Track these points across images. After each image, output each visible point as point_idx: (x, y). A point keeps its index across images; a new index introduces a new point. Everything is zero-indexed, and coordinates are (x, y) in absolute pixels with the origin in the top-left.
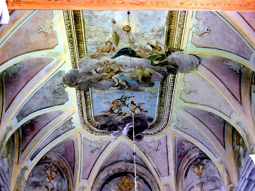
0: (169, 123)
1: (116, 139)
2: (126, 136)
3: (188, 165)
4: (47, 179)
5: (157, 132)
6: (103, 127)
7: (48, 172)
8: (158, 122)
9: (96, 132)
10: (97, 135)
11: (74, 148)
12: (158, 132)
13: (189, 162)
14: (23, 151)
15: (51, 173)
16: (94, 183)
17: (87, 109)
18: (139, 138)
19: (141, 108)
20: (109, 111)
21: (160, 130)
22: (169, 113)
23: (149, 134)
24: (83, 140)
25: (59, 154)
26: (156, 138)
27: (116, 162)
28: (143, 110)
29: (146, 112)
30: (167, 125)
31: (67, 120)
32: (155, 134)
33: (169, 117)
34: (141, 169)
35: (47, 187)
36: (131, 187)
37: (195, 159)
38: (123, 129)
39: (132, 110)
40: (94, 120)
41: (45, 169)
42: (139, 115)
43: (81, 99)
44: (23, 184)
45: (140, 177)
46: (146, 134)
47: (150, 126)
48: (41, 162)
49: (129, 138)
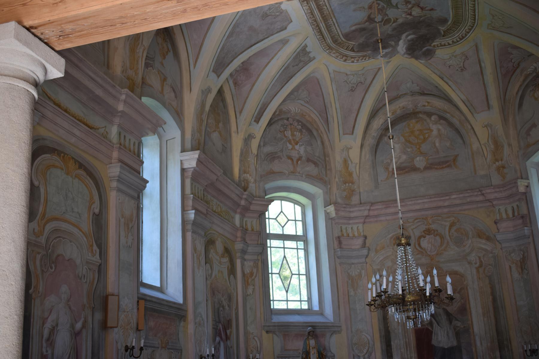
0: (477, 20)
1: (388, 62)
2: (404, 54)
3: (523, 88)
4: (288, 145)
5: (459, 40)
6: (362, 47)
7: (288, 133)
8: (457, 23)
9: (352, 58)
10: (355, 62)
11: (321, 89)
12: (461, 39)
13: (524, 81)
14: (241, 112)
15: (293, 135)
16: (364, 138)
17: (328, 27)
18: (429, 54)
19: (421, 5)
20: (367, 21)
21: (464, 35)
22: (474, 6)
23: (445, 45)
24: (332, 75)
25: (299, 101)
26: (458, 49)
27: (396, 98)
28: (427, 9)
29: (432, 10)
30: (474, 25)
31: (298, 50)
32: (455, 43)
33: (474, 12)
34: (438, 103)
35: (290, 158)
36: (427, 137)
37: (535, 74)
38: (397, 44)
39: (406, 12)
40: (344, 39)
41: (282, 129)
42: (421, 17)
43: (312, 14)
44: (252, 160)
45: (441, 118)
46: (439, 45)
47: (444, 32)
48: (274, 120)
49: (410, 57)
